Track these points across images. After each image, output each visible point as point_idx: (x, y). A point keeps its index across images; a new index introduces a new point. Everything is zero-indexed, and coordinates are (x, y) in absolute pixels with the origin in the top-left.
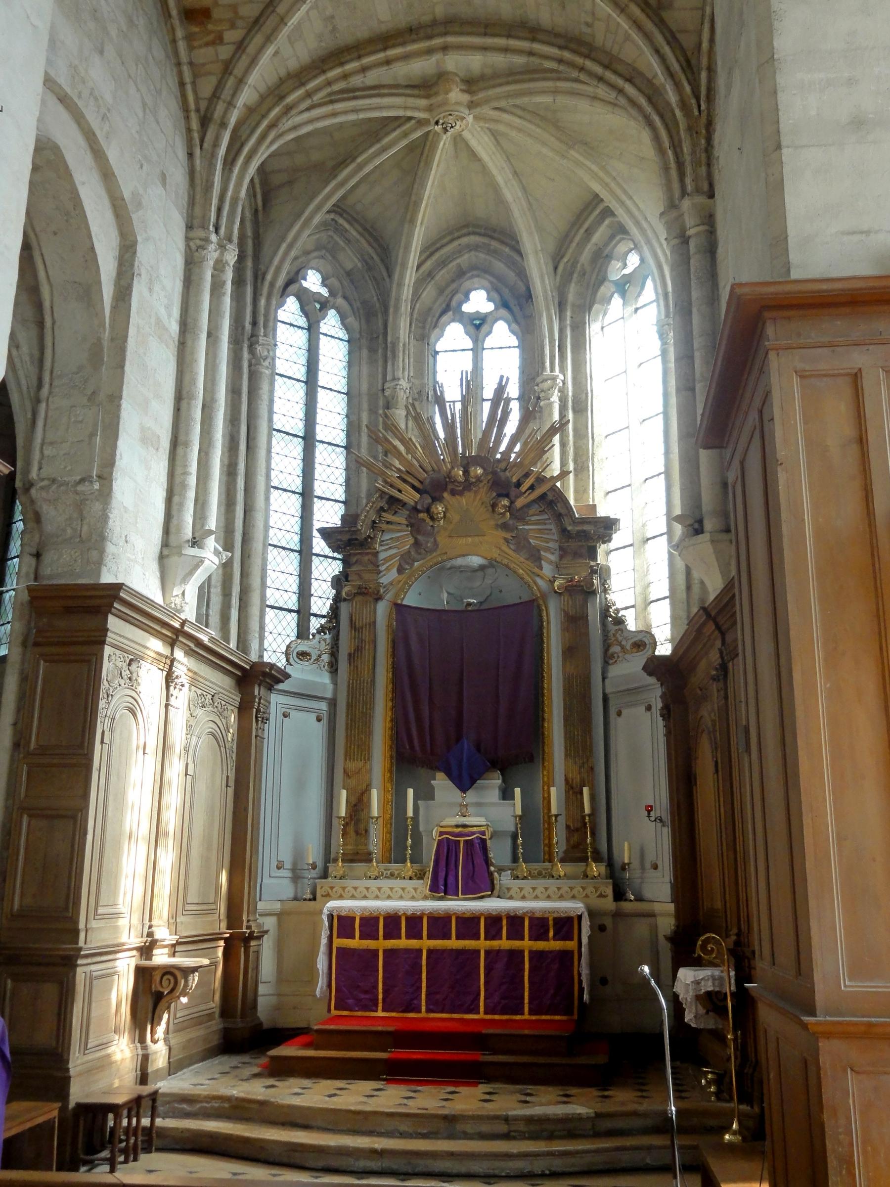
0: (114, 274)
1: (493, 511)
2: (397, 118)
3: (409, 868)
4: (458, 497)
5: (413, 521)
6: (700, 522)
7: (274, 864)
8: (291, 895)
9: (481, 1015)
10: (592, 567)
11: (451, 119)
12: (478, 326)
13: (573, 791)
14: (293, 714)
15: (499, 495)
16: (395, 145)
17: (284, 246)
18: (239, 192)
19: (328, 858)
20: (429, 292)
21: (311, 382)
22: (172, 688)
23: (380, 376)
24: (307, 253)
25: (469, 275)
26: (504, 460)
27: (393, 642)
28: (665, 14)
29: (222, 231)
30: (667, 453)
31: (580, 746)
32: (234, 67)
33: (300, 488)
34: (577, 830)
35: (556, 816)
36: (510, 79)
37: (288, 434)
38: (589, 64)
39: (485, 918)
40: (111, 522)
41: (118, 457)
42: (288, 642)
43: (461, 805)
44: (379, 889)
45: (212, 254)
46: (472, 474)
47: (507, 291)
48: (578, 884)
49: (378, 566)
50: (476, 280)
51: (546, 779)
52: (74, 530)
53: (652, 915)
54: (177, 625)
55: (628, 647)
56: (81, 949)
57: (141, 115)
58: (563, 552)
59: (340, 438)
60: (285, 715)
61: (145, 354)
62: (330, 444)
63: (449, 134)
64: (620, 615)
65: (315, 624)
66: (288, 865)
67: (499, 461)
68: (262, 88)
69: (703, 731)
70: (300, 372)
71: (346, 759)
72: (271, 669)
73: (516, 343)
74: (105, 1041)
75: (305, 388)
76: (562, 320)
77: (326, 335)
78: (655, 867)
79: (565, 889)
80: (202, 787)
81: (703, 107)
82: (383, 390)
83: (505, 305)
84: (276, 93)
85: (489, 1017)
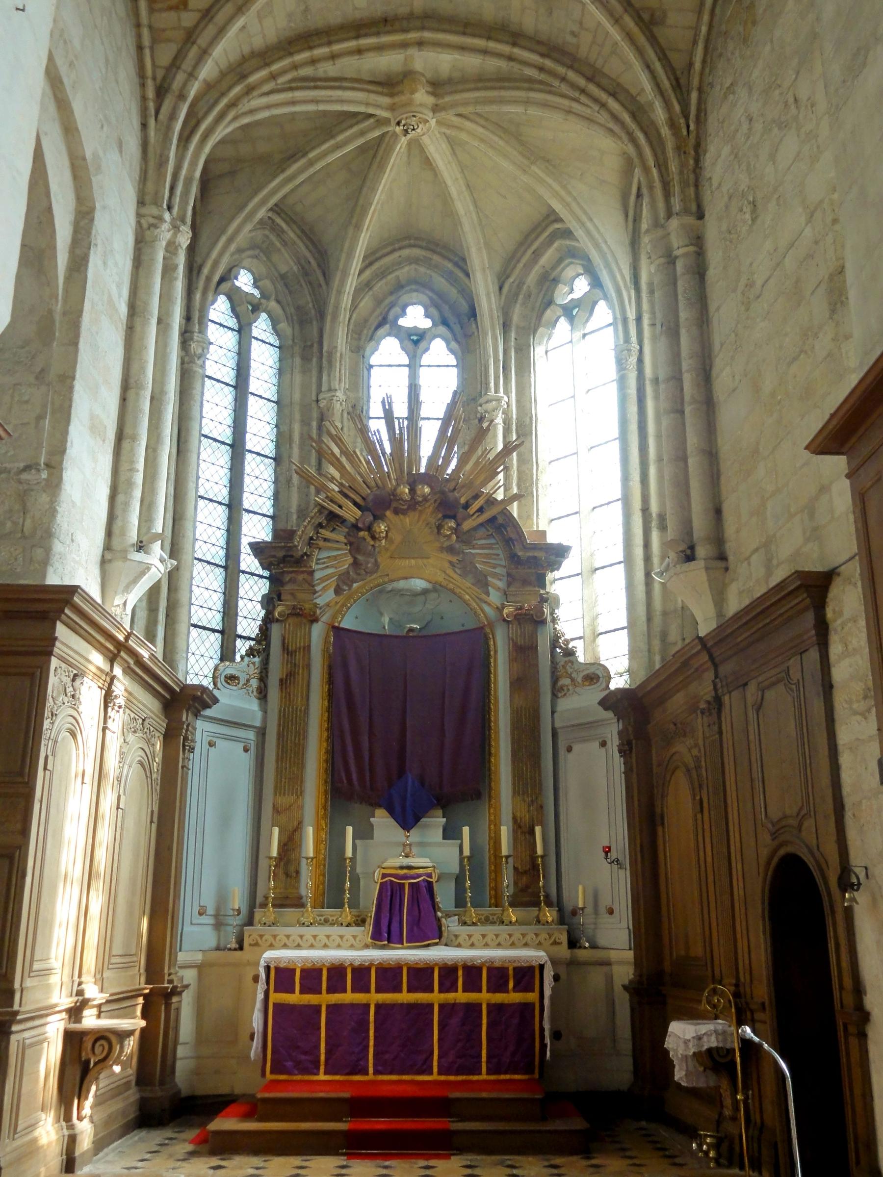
0: (69, 240)
1: (439, 532)
2: (355, 114)
3: (347, 914)
4: (402, 516)
5: (352, 539)
6: (692, 548)
7: (196, 909)
8: (213, 943)
9: (435, 1077)
10: (541, 595)
11: (413, 121)
12: (415, 342)
13: (523, 831)
14: (219, 742)
15: (445, 517)
16: (349, 143)
17: (223, 239)
18: (194, 171)
19: (253, 903)
20: (366, 303)
21: (241, 386)
22: (110, 709)
23: (314, 387)
24: (240, 251)
25: (408, 288)
26: (454, 479)
27: (330, 667)
28: (655, 30)
29: (175, 210)
30: (626, 478)
31: (528, 782)
32: (198, 37)
33: (227, 498)
34: (525, 872)
35: (507, 857)
36: (480, 85)
37: (215, 440)
38: (571, 75)
39: (440, 969)
40: (59, 518)
41: (69, 444)
42: (212, 664)
43: (404, 845)
44: (315, 937)
45: (164, 233)
46: (419, 492)
47: (447, 307)
48: (530, 930)
49: (313, 586)
50: (415, 294)
51: (492, 818)
52: (15, 523)
53: (608, 963)
54: (121, 637)
55: (579, 680)
56: (17, 1013)
57: (104, 70)
58: (511, 579)
59: (269, 449)
60: (211, 744)
61: (97, 333)
62: (258, 454)
63: (409, 136)
64: (570, 646)
65: (242, 647)
66: (211, 911)
67: (447, 480)
68: (223, 64)
69: (677, 768)
70: (229, 376)
71: (275, 794)
72: (202, 693)
73: (455, 363)
74: (33, 1122)
75: (234, 393)
77: (256, 339)
78: (611, 912)
79: (517, 936)
80: (130, 823)
81: (692, 127)
82: (317, 401)
83: (445, 323)
84: (238, 71)
85: (443, 1078)
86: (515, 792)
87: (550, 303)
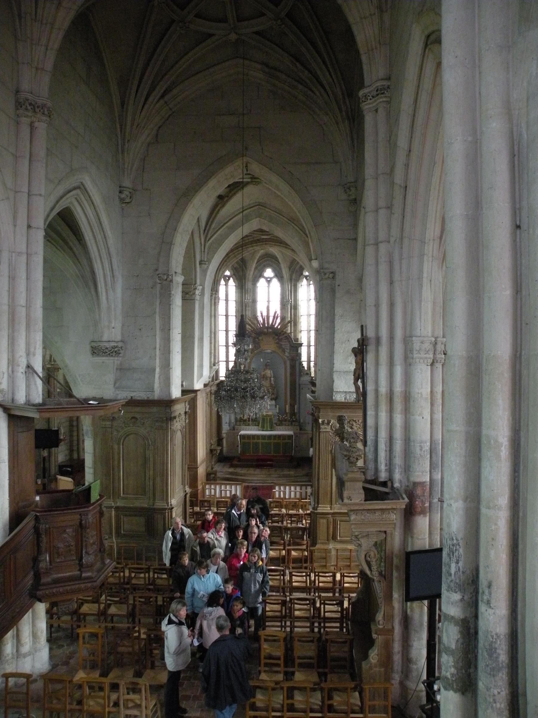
12: (269, 281)
20: (257, 271)
66: (228, 422)
76: (291, 284)
86: (291, 398)
87: (302, 274)
